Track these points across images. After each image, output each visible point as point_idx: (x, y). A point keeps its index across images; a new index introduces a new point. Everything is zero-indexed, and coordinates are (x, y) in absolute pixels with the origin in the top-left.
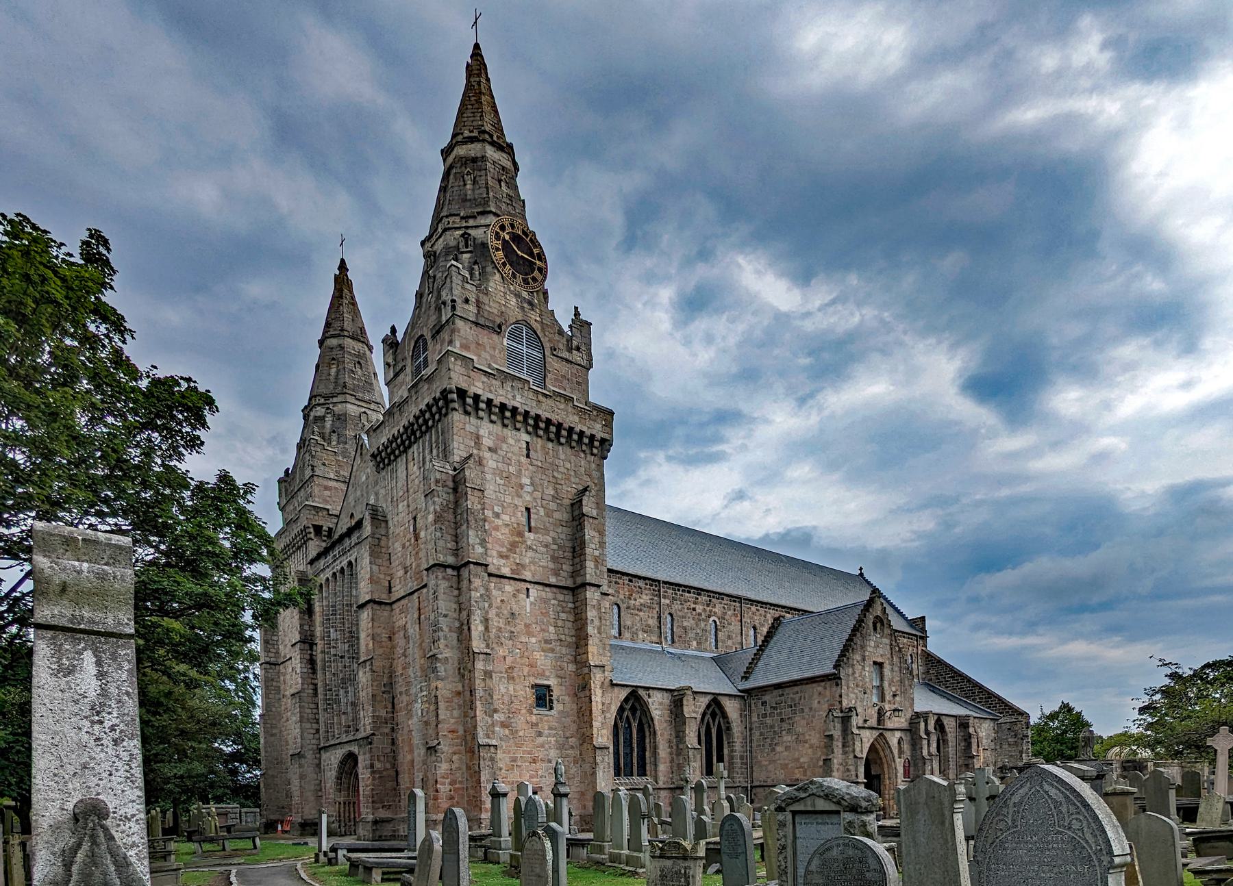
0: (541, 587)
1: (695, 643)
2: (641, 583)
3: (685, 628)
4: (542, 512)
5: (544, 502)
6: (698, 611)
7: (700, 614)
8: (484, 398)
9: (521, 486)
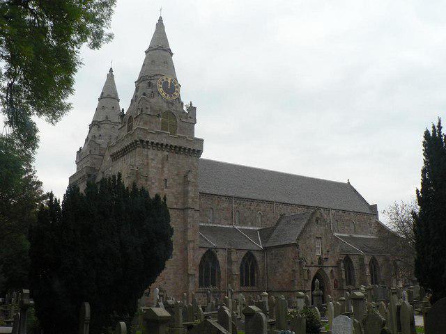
2: (223, 198)
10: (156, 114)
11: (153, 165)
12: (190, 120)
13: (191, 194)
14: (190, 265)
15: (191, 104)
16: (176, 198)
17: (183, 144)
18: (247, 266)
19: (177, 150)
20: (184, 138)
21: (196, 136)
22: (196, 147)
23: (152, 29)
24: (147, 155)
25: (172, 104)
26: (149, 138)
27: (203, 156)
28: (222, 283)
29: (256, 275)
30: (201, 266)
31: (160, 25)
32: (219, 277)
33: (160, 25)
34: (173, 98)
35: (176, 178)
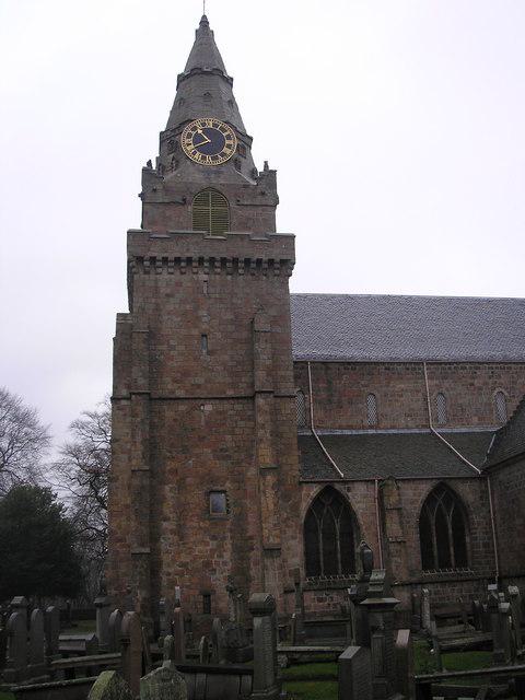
0: (217, 401)
1: (475, 419)
4: (219, 335)
5: (221, 327)
7: (480, 389)
10: (178, 199)
11: (170, 307)
13: (264, 359)
17: (244, 251)
18: (441, 518)
19: (230, 264)
20: (242, 237)
21: (283, 226)
22: (277, 255)
24: (157, 288)
25: (218, 173)
29: (468, 539)
31: (204, 32)
33: (204, 32)
34: (221, 160)
35: (231, 328)
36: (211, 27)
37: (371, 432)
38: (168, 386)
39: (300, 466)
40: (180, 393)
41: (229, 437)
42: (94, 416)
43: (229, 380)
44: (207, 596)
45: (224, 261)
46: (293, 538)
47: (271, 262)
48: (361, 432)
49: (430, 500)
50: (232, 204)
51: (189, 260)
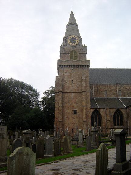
1: (127, 96)
2: (112, 85)
3: (124, 93)
4: (75, 80)
6: (128, 88)
8: (64, 65)
9: (71, 77)
11: (66, 75)
12: (84, 53)
14: (84, 117)
15: (85, 45)
16: (78, 88)
17: (80, 63)
18: (118, 116)
20: (80, 61)
21: (88, 58)
22: (87, 64)
23: (69, 17)
25: (75, 47)
26: (63, 64)
27: (91, 67)
28: (103, 124)
29: (123, 120)
30: (92, 117)
31: (72, 14)
32: (102, 121)
34: (76, 44)
35: (78, 79)
36: (73, 13)
37: (106, 98)
38: (66, 90)
39: (91, 106)
40: (68, 91)
41: (77, 100)
42: (49, 91)
43: (77, 89)
44: (73, 130)
45: (76, 65)
46: (89, 119)
47: (85, 65)
48: (103, 98)
49: (116, 112)
50: (78, 53)
51: (70, 65)
